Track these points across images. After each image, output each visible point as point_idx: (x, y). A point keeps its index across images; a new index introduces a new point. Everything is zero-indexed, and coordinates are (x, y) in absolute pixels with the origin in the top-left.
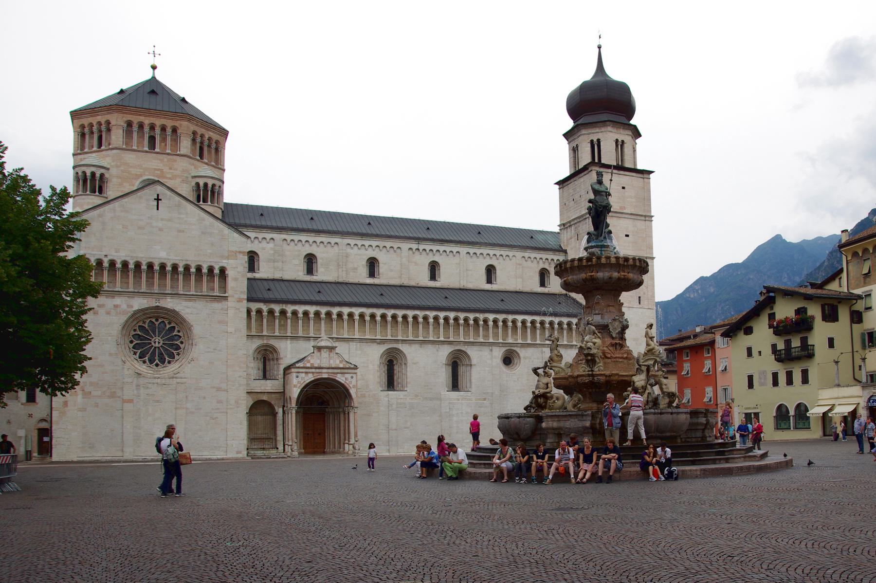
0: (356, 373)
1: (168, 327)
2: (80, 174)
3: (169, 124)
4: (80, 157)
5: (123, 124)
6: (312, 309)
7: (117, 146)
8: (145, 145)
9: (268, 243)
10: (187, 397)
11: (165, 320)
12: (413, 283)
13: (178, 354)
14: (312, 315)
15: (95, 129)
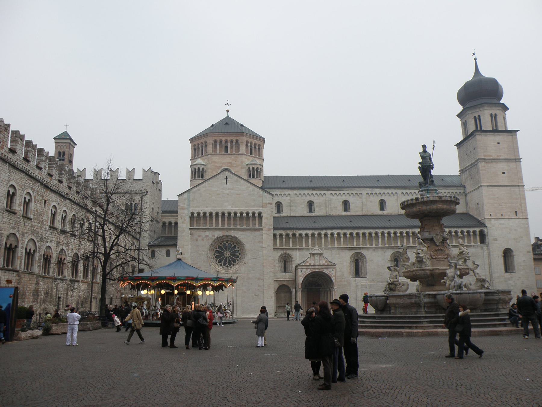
0: (335, 268)
1: (232, 246)
2: (193, 169)
3: (234, 139)
4: (193, 161)
5: (212, 142)
6: (310, 232)
7: (210, 153)
10: (242, 283)
11: (231, 242)
12: (370, 213)
13: (238, 260)
14: (310, 236)
15: (200, 146)
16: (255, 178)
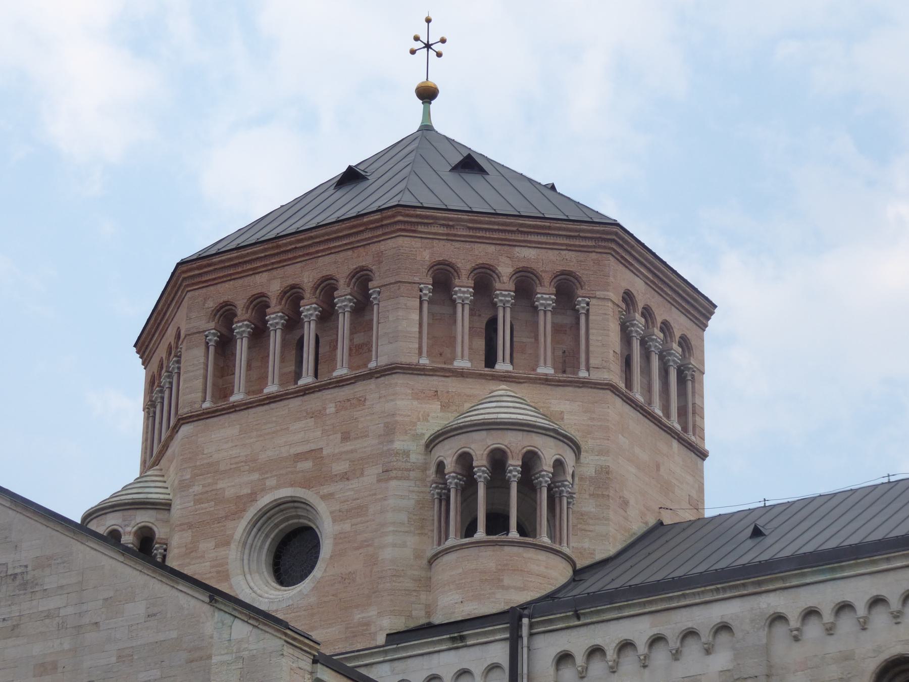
8: (270, 378)
9: (708, 652)
16: (481, 534)
